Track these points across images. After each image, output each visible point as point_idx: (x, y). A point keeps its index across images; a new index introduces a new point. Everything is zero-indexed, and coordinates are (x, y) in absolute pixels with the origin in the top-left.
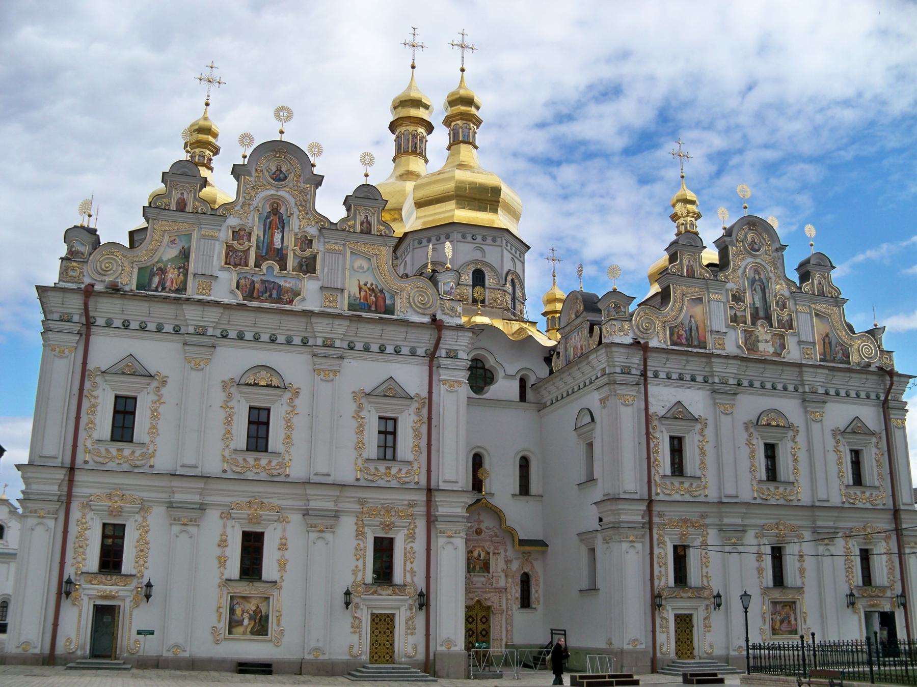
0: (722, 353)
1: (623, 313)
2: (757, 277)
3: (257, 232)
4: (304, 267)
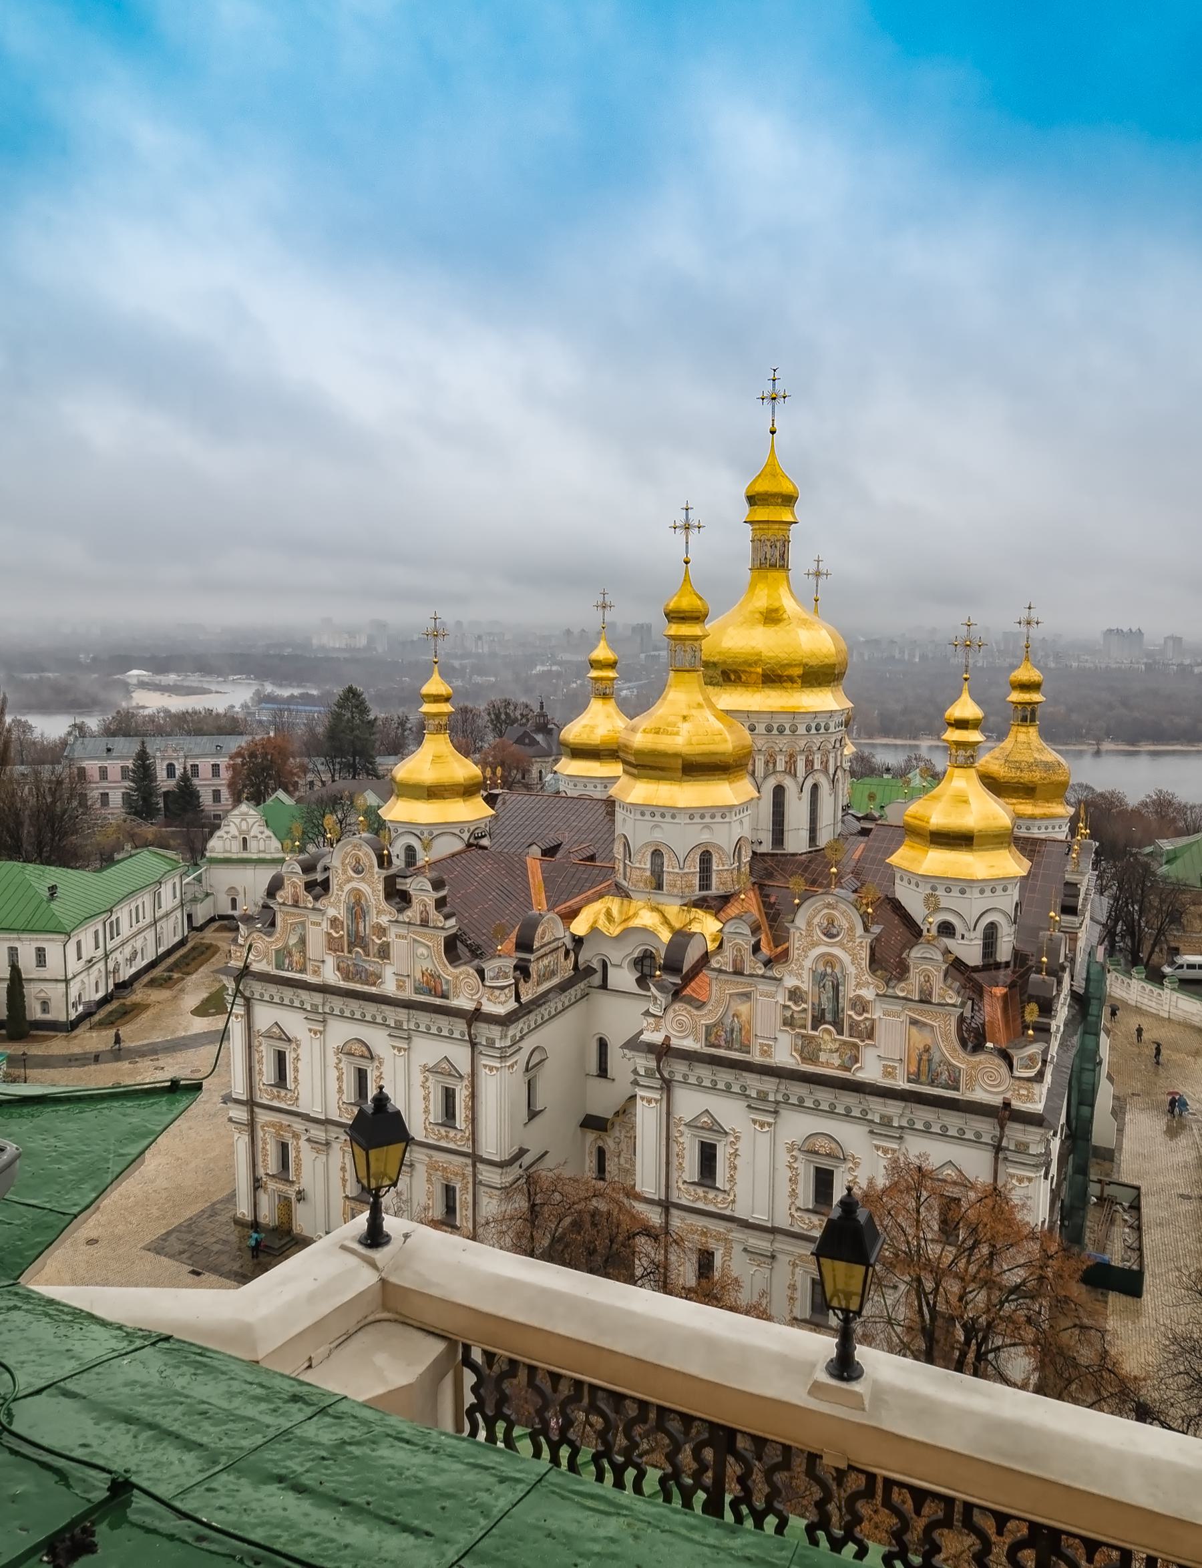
2: (829, 970)
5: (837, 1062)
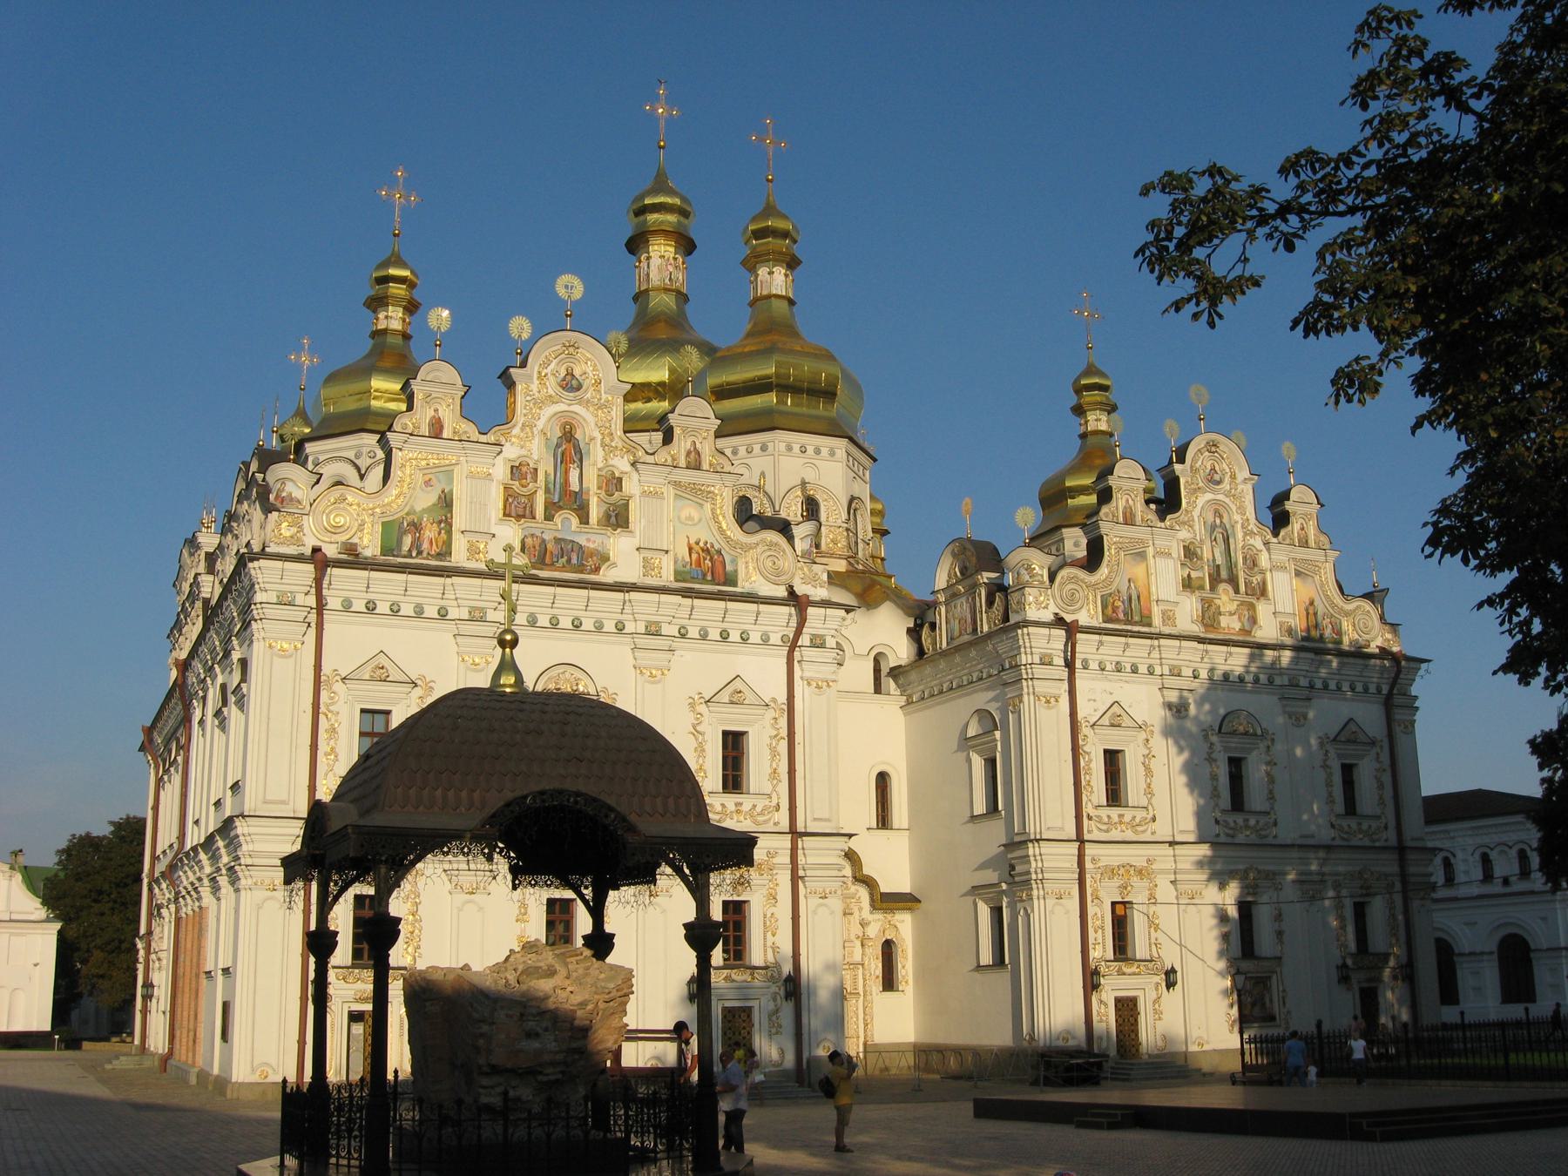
0: (1174, 631)
1: (1040, 577)
2: (1218, 521)
3: (546, 467)
4: (613, 519)
5: (1237, 626)
